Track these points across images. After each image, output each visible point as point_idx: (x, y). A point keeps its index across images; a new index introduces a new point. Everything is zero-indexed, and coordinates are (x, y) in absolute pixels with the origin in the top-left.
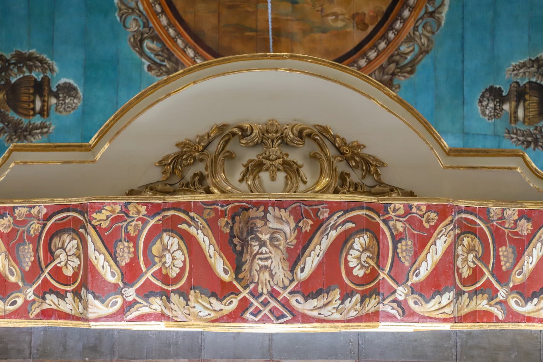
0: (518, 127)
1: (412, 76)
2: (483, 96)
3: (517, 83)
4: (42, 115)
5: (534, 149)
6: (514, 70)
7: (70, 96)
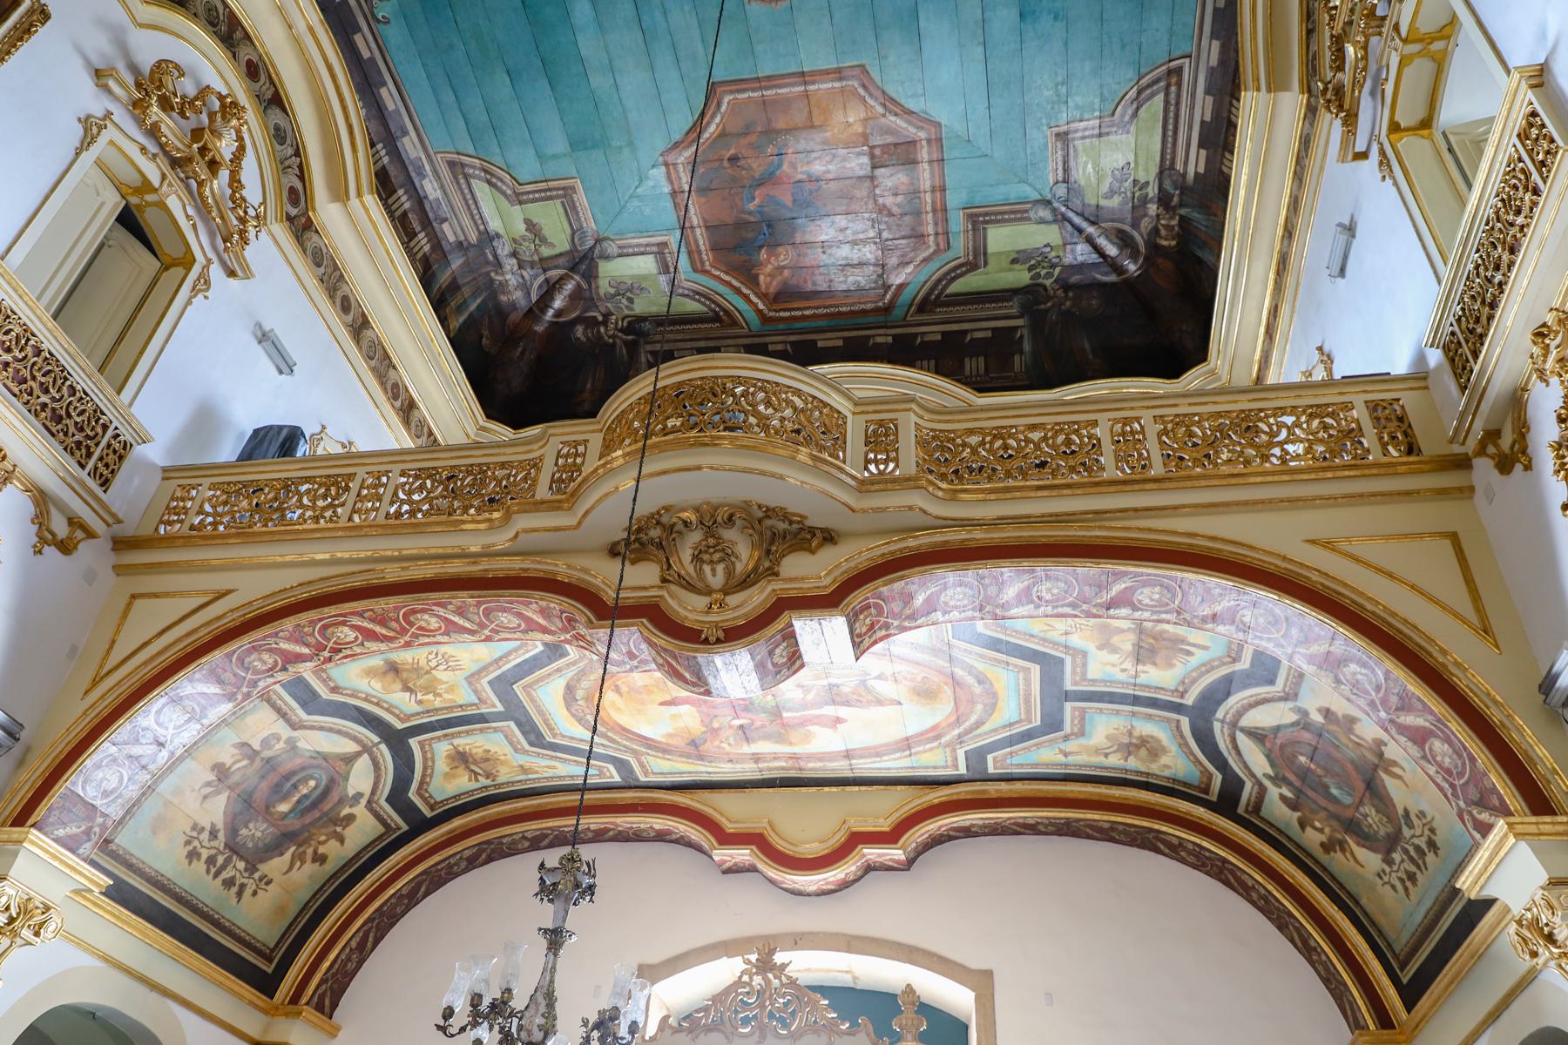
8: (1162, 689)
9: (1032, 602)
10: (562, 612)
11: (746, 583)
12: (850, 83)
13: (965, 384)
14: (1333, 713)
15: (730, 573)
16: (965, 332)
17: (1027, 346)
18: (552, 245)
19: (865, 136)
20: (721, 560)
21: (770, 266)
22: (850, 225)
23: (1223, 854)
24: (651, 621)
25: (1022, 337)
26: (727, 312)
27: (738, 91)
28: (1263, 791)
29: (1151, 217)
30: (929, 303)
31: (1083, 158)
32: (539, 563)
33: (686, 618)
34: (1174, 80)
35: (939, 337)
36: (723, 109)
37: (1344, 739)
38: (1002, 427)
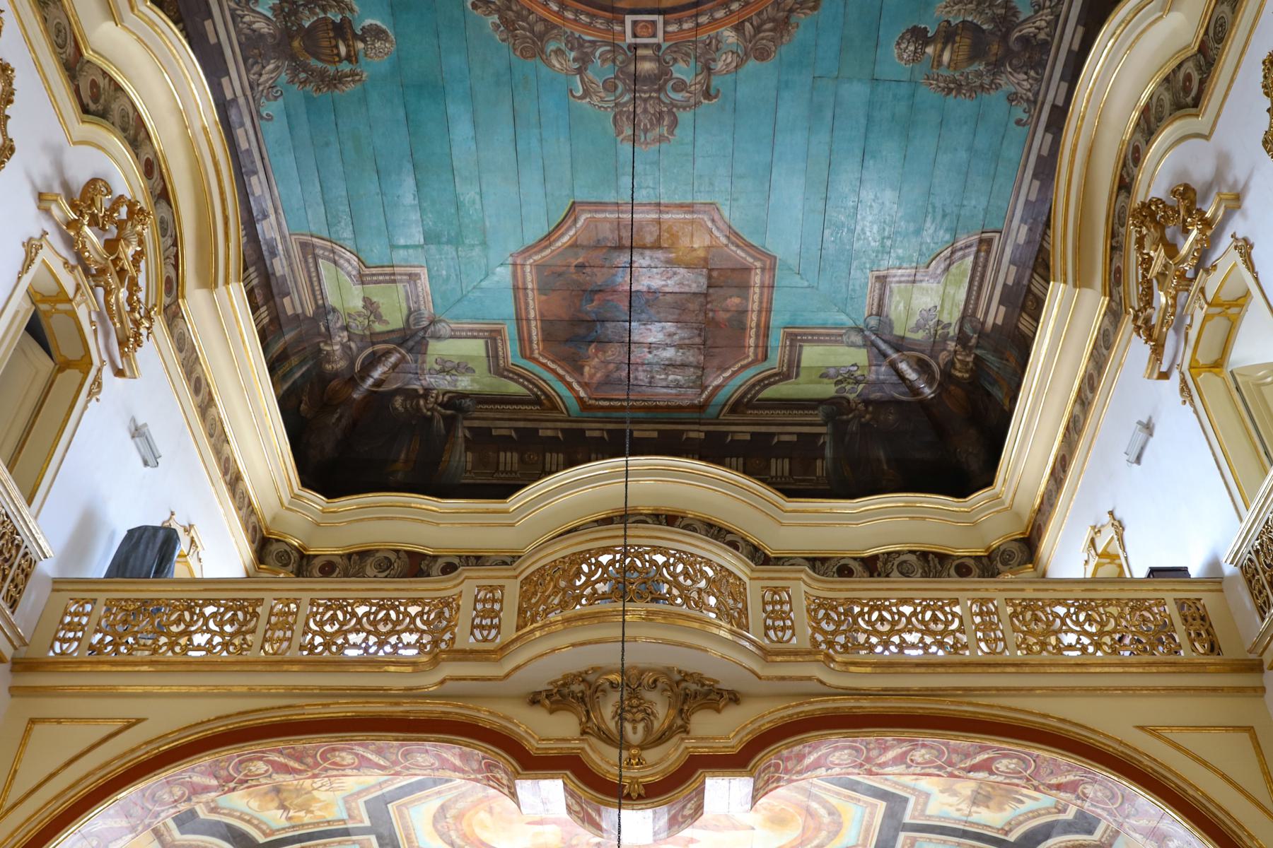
0: (940, 73)
1: (816, 13)
2: (902, 38)
3: (948, 22)
4: (350, 62)
5: (956, 97)
6: (946, 7)
7: (379, 40)
9: (905, 763)
10: (484, 758)
11: (661, 739)
12: (701, 216)
13: (769, 484)
15: (648, 729)
16: (773, 434)
17: (828, 453)
18: (387, 322)
19: (706, 260)
20: (643, 719)
21: (596, 360)
22: (679, 331)
24: (574, 772)
25: (824, 443)
26: (548, 396)
27: (596, 211)
29: (949, 351)
30: (739, 406)
31: (896, 298)
32: (460, 707)
33: (609, 772)
34: (984, 248)
35: (748, 437)
36: (579, 224)
38: (879, 599)
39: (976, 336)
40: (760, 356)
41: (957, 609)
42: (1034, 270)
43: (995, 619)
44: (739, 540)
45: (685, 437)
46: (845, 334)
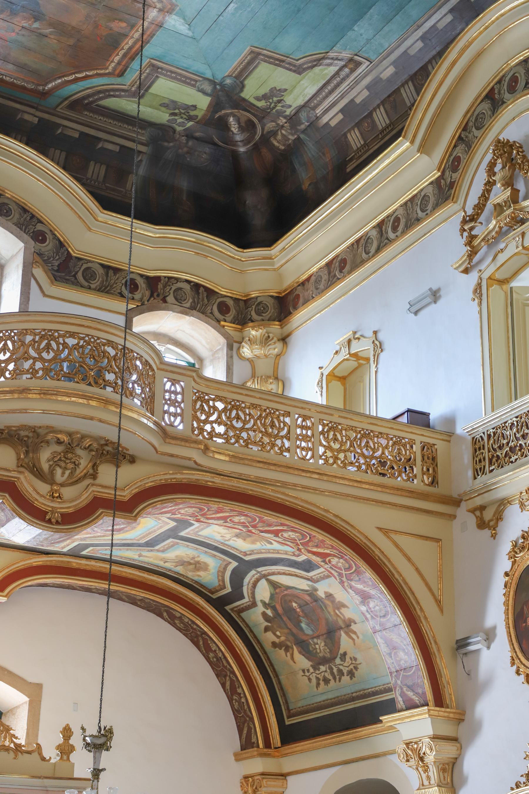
8: (237, 549)
13: (83, 184)
14: (333, 597)
16: (99, 139)
23: (205, 629)
25: (141, 161)
28: (254, 604)
29: (278, 124)
33: (37, 500)
34: (351, 66)
35: (77, 135)
37: (330, 610)
38: (238, 401)
39: (307, 124)
40: (117, 72)
41: (287, 420)
42: (383, 103)
43: (309, 433)
44: (48, 232)
45: (19, 116)
46: (200, 81)
